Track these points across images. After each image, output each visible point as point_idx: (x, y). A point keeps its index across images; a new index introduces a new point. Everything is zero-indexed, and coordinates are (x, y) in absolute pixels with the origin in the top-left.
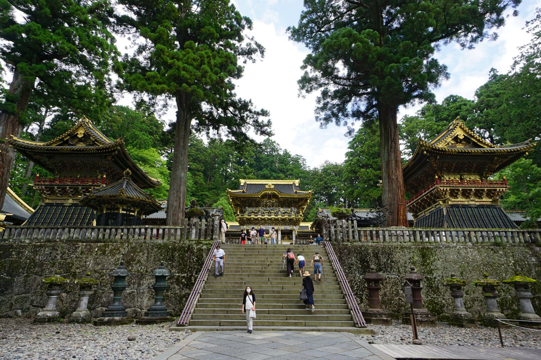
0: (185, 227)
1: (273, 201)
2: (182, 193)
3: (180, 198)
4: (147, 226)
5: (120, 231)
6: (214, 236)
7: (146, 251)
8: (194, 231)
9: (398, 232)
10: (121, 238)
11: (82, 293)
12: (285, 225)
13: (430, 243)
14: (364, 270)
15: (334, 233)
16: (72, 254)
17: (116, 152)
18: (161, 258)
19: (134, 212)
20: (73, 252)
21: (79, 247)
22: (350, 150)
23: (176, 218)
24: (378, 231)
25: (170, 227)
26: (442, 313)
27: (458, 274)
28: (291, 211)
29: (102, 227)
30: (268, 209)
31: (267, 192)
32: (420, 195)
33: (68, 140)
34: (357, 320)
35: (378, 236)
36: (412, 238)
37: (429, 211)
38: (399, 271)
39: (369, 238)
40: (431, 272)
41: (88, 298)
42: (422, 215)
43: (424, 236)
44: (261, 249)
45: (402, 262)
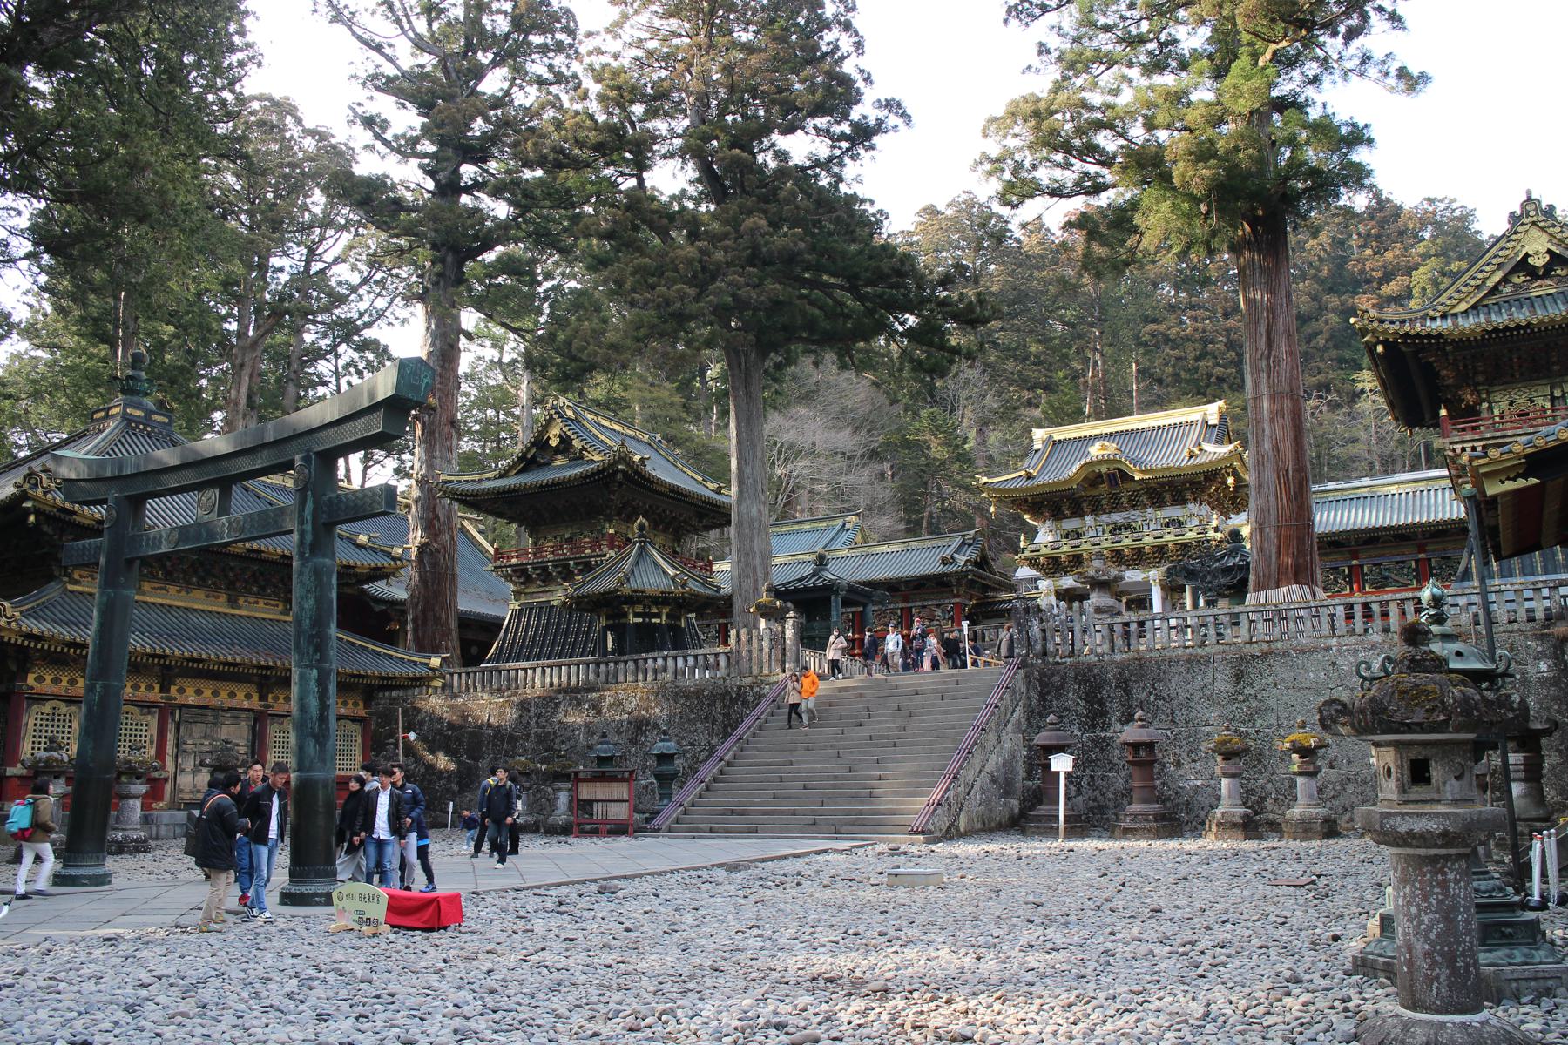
3: (754, 569)
19: (658, 616)
33: (534, 456)
38: (1173, 722)
39: (1119, 642)
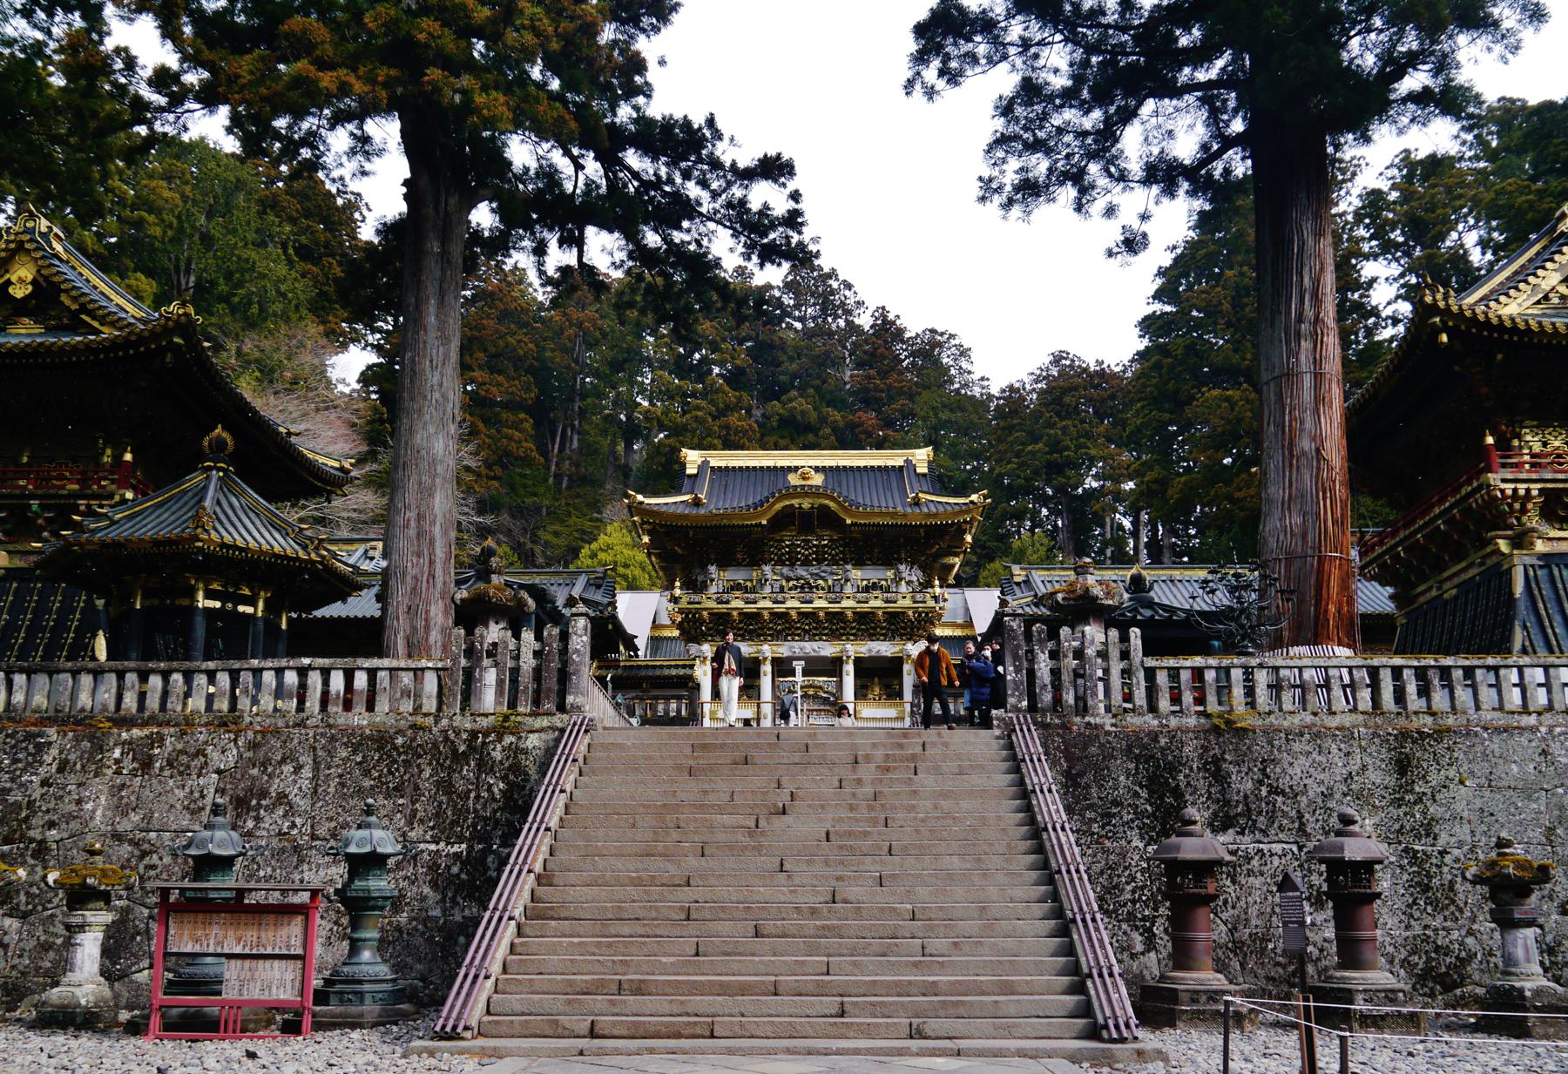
0: (455, 660)
1: (820, 538)
2: (439, 520)
3: (432, 542)
4: (306, 661)
5: (201, 680)
6: (570, 699)
7: (306, 759)
8: (491, 677)
9: (1307, 674)
10: (209, 708)
11: (79, 920)
12: (872, 636)
13: (1433, 714)
14: (1163, 825)
15: (1047, 679)
16: (24, 770)
17: (169, 357)
18: (367, 783)
19: (252, 601)
20: (29, 764)
21: (50, 744)
22: (1158, 307)
23: (420, 624)
24: (1227, 670)
25: (395, 664)
26: (1461, 985)
27: (1537, 834)
28: (898, 580)
29: (132, 664)
30: (801, 572)
31: (795, 502)
32: (1422, 516)
34: (1108, 1013)
35: (1224, 690)
36: (1365, 695)
37: (1456, 581)
38: (1302, 830)
39: (1188, 698)
40: (1428, 829)
41: (100, 936)
42: (1428, 596)
43: (1411, 688)
44: (756, 746)
45: (1314, 790)
